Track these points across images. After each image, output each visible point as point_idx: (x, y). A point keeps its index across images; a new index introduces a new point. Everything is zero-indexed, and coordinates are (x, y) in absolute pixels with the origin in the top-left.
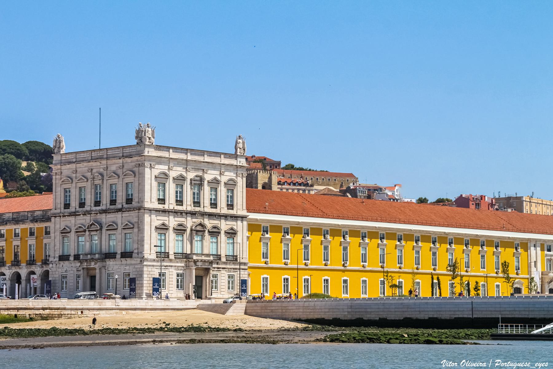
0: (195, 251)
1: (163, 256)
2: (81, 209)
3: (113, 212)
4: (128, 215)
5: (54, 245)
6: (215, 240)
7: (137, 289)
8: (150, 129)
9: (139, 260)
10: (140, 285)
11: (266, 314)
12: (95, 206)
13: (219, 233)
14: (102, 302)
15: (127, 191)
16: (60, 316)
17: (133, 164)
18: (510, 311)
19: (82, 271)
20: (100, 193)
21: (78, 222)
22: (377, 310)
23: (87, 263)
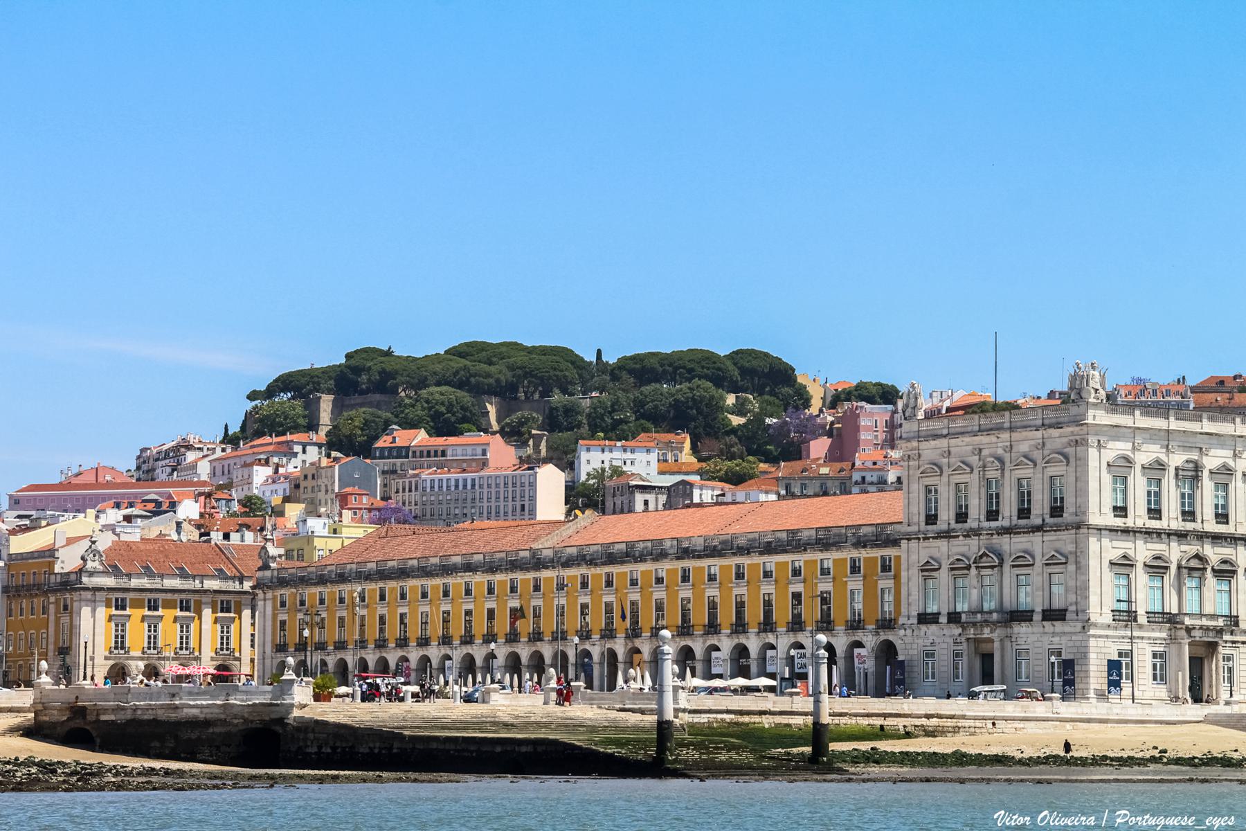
0: (1187, 610)
1: (1126, 616)
2: (960, 525)
6: (1225, 587)
7: (1077, 680)
8: (1096, 373)
9: (1079, 625)
10: (1082, 674)
12: (988, 520)
13: (1234, 572)
14: (1028, 707)
16: (956, 730)
17: (1065, 440)
19: (965, 644)
20: (997, 495)
21: (955, 550)
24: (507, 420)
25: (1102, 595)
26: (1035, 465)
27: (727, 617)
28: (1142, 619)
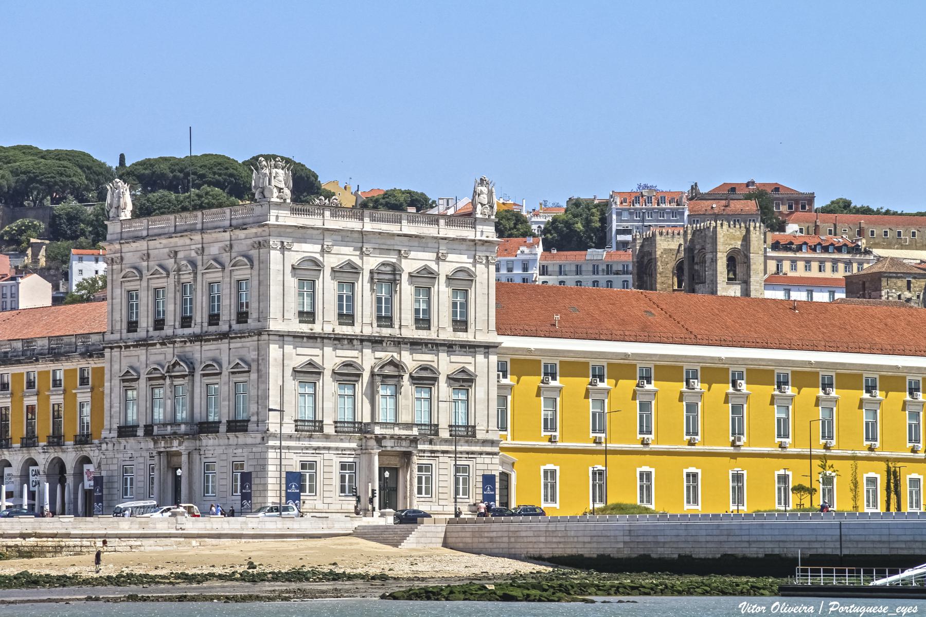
0: (381, 418)
1: (312, 427)
2: (157, 333)
3: (214, 340)
4: (239, 345)
6: (425, 395)
9: (259, 436)
10: (261, 488)
11: (481, 546)
12: (183, 327)
13: (435, 379)
15: (239, 296)
16: (57, 550)
17: (249, 242)
18: (906, 542)
19: (156, 458)
21: (153, 358)
22: (674, 539)
23: (166, 442)
24: (7, 228)
26: (223, 268)
28: (329, 430)
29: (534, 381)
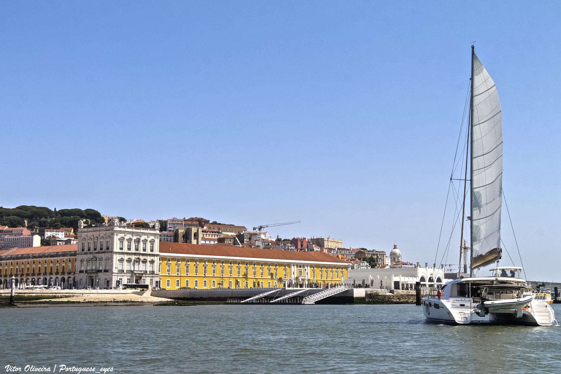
5: (79, 266)
16: (73, 296)
25: (116, 265)
27: (43, 271)
28: (125, 272)
29: (166, 262)
